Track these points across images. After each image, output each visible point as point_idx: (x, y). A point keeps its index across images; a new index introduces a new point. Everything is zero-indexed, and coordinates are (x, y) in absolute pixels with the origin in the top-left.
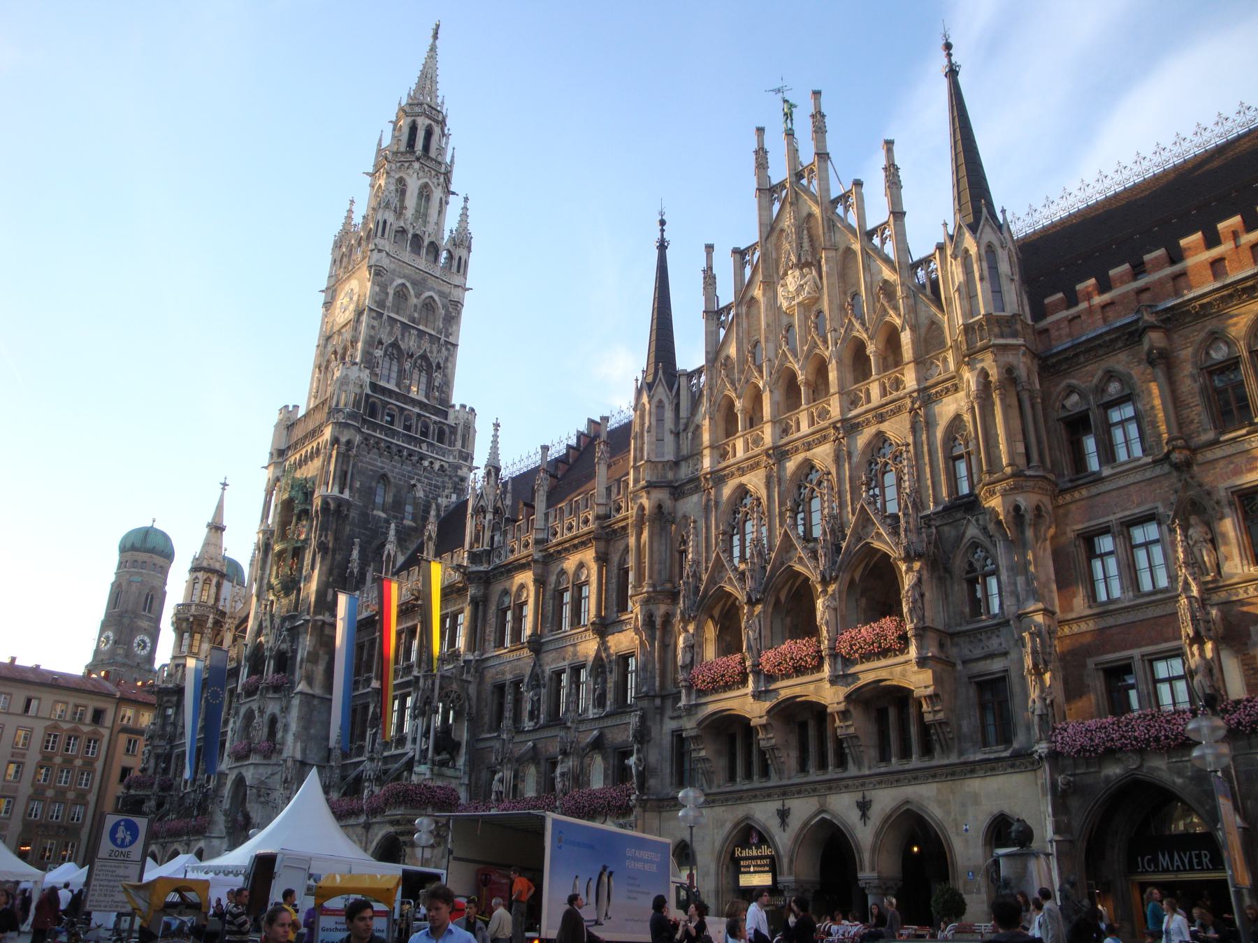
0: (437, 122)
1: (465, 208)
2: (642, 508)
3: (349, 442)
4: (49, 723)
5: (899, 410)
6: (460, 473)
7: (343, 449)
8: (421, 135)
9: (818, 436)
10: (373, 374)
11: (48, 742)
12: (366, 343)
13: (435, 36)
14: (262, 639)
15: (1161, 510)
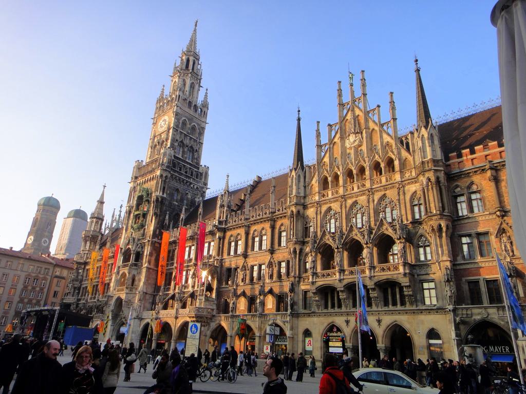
0: (196, 58)
1: (206, 93)
2: (292, 211)
3: (166, 177)
4: (27, 273)
6: (203, 190)
7: (164, 179)
8: (191, 63)
9: (361, 193)
10: (175, 152)
11: (26, 281)
12: (171, 140)
13: (196, 26)
15: (491, 230)
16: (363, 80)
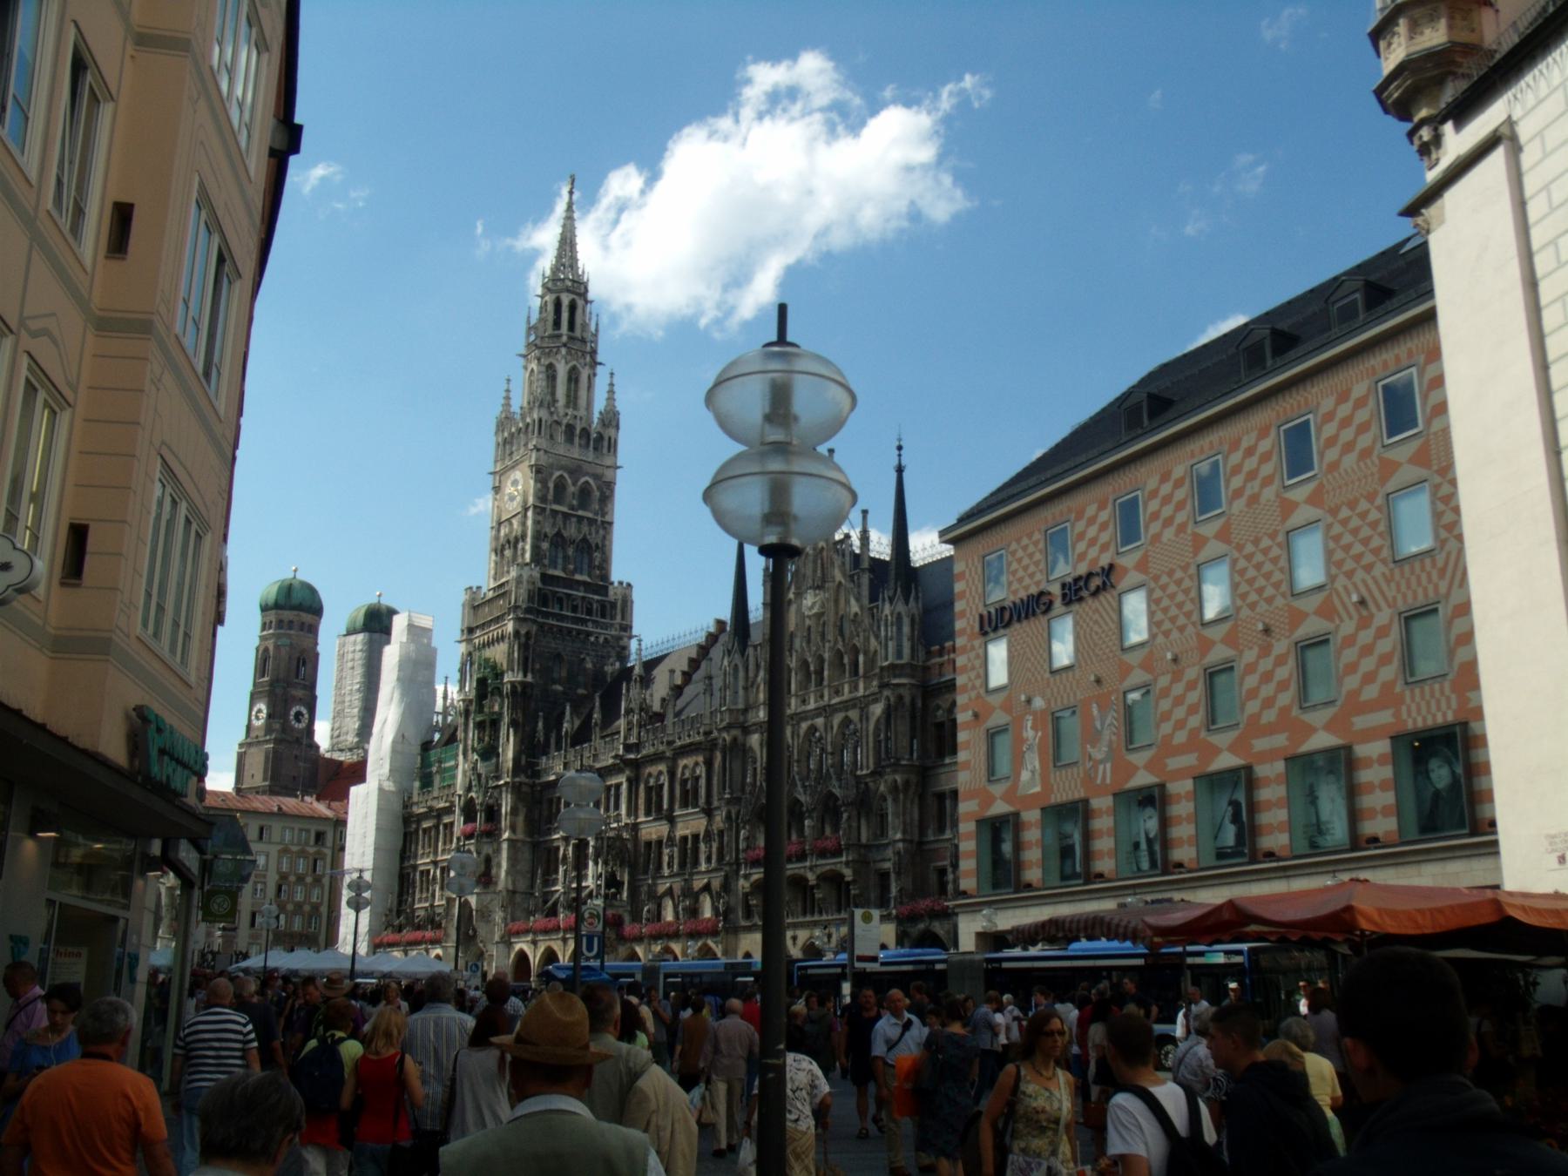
1: (612, 385)
3: (528, 633)
5: (854, 706)
7: (523, 640)
8: (565, 315)
14: (473, 794)
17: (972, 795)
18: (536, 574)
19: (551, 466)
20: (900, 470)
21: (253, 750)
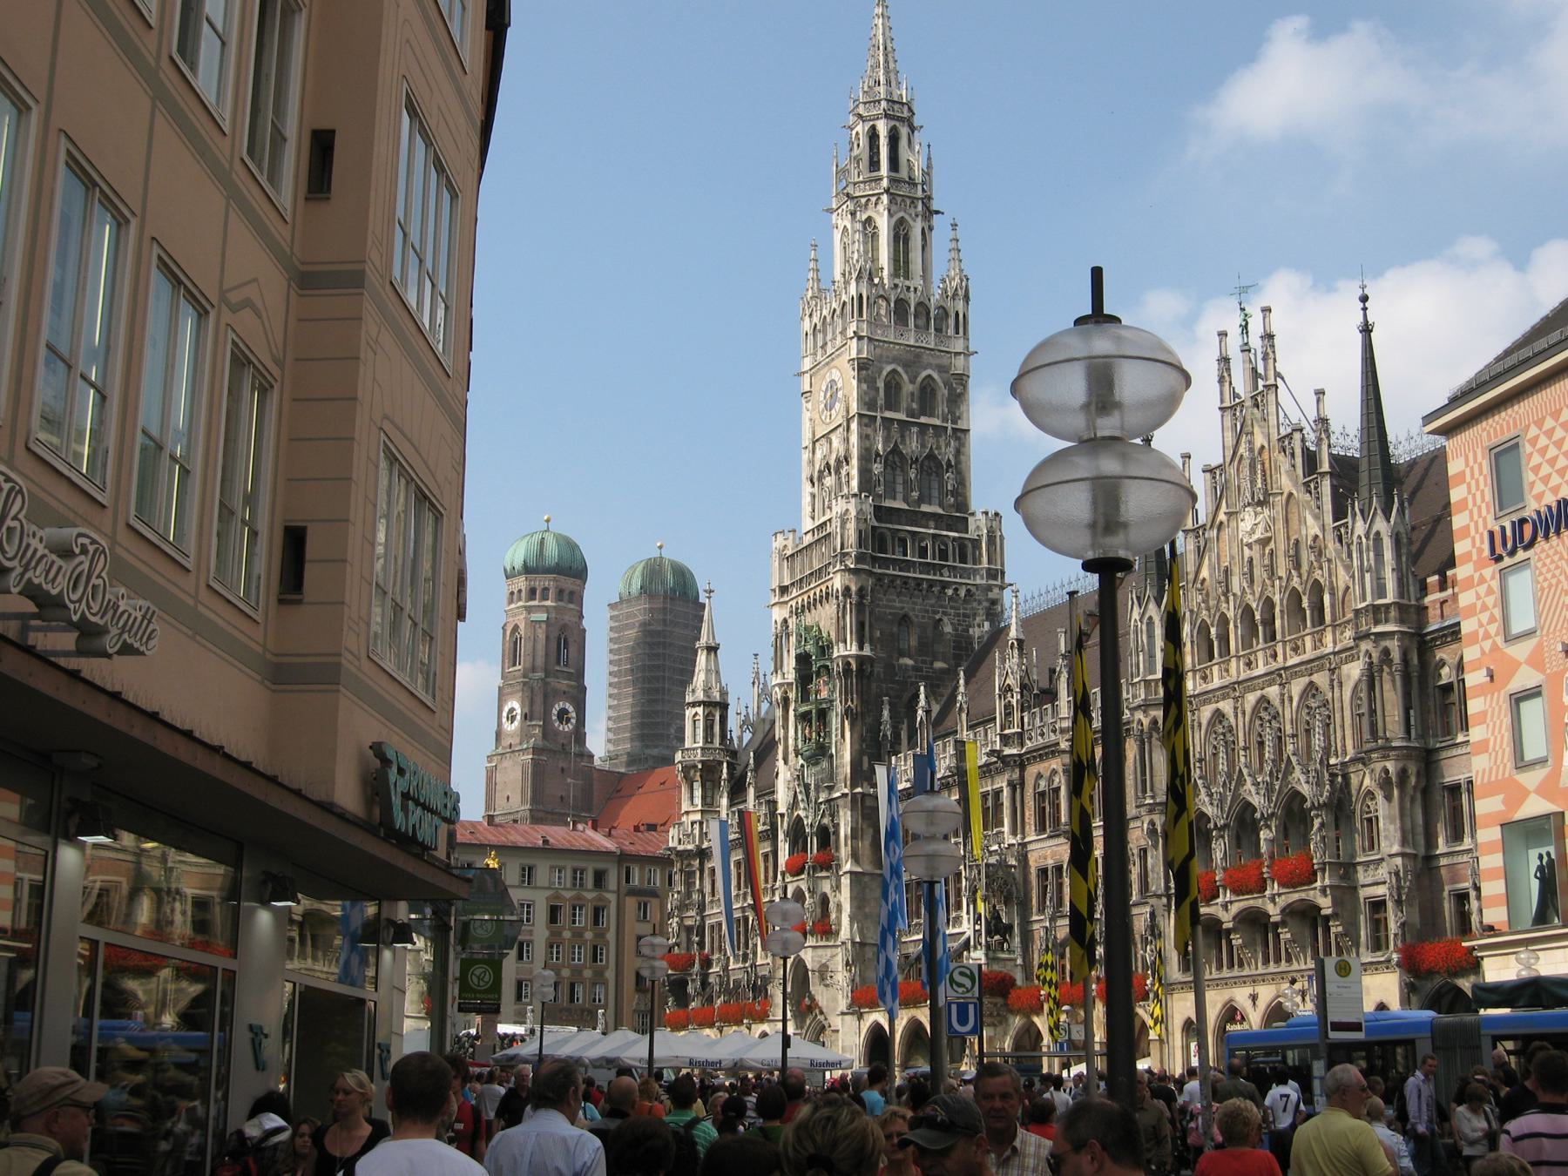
3: (861, 591)
5: (1321, 669)
12: (861, 458)
16: (1269, 337)
17: (1492, 790)
18: (868, 507)
19: (880, 359)
20: (1366, 330)
21: (507, 763)
